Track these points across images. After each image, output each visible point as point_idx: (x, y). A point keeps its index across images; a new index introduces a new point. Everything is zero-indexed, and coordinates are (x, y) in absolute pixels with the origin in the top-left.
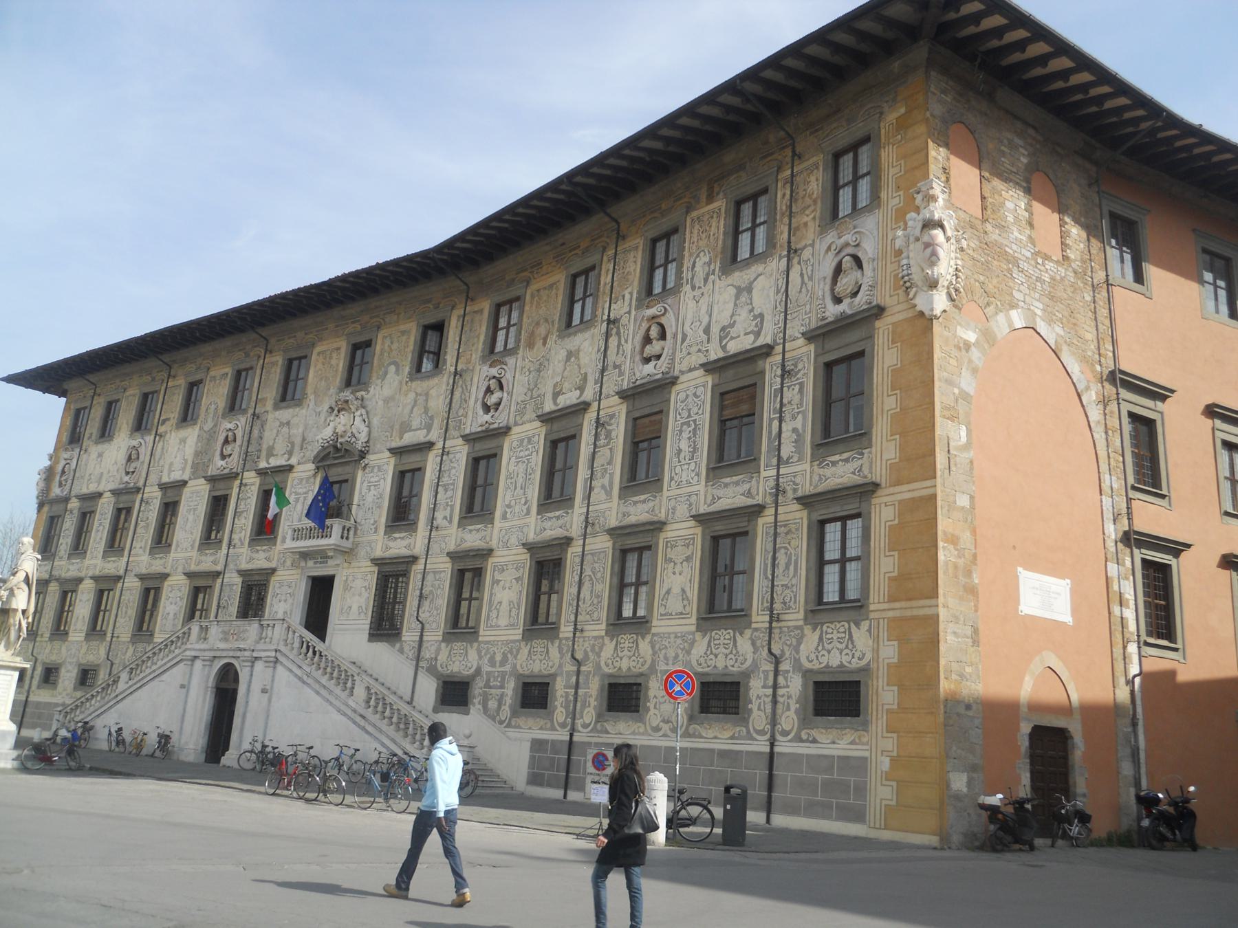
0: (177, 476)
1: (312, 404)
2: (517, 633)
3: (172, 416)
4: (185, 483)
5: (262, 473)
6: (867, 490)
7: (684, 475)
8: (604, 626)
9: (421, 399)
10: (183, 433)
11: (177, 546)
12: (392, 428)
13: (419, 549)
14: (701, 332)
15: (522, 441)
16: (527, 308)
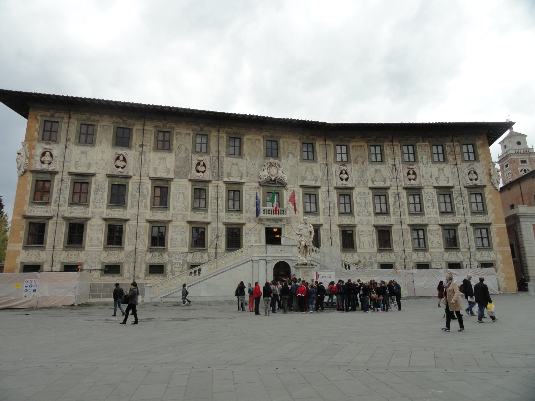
0: (164, 175)
1: (249, 159)
2: (375, 250)
3: (148, 145)
4: (171, 180)
5: (226, 183)
6: (489, 224)
7: (432, 213)
8: (411, 249)
9: (309, 170)
10: (160, 154)
11: (174, 208)
12: (297, 177)
13: (321, 222)
14: (429, 176)
15: (360, 193)
16: (351, 150)
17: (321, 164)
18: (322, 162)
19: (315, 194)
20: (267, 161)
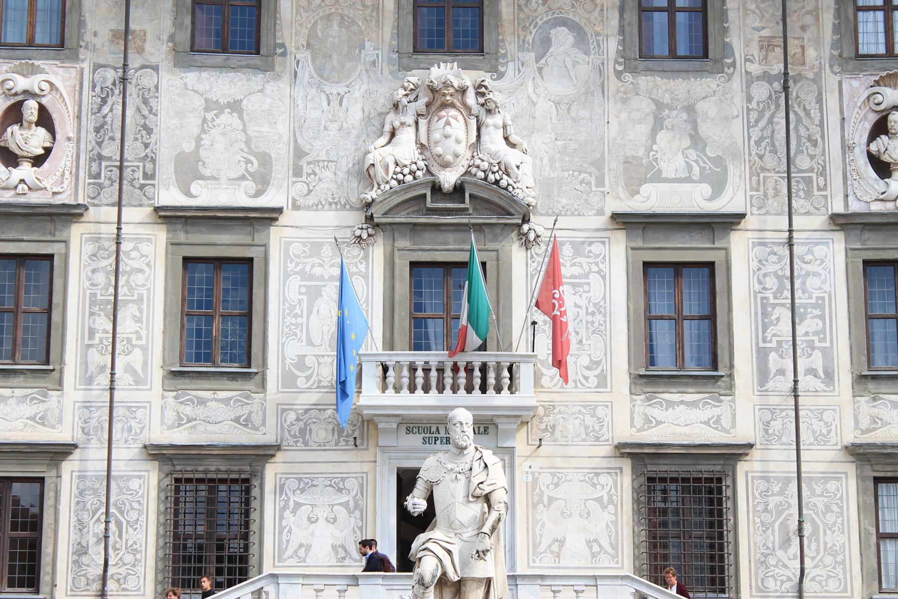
1: (307, 71)
9: (678, 118)
12: (599, 164)
17: (750, 79)
18: (755, 68)
19: (711, 265)
20: (414, 78)
